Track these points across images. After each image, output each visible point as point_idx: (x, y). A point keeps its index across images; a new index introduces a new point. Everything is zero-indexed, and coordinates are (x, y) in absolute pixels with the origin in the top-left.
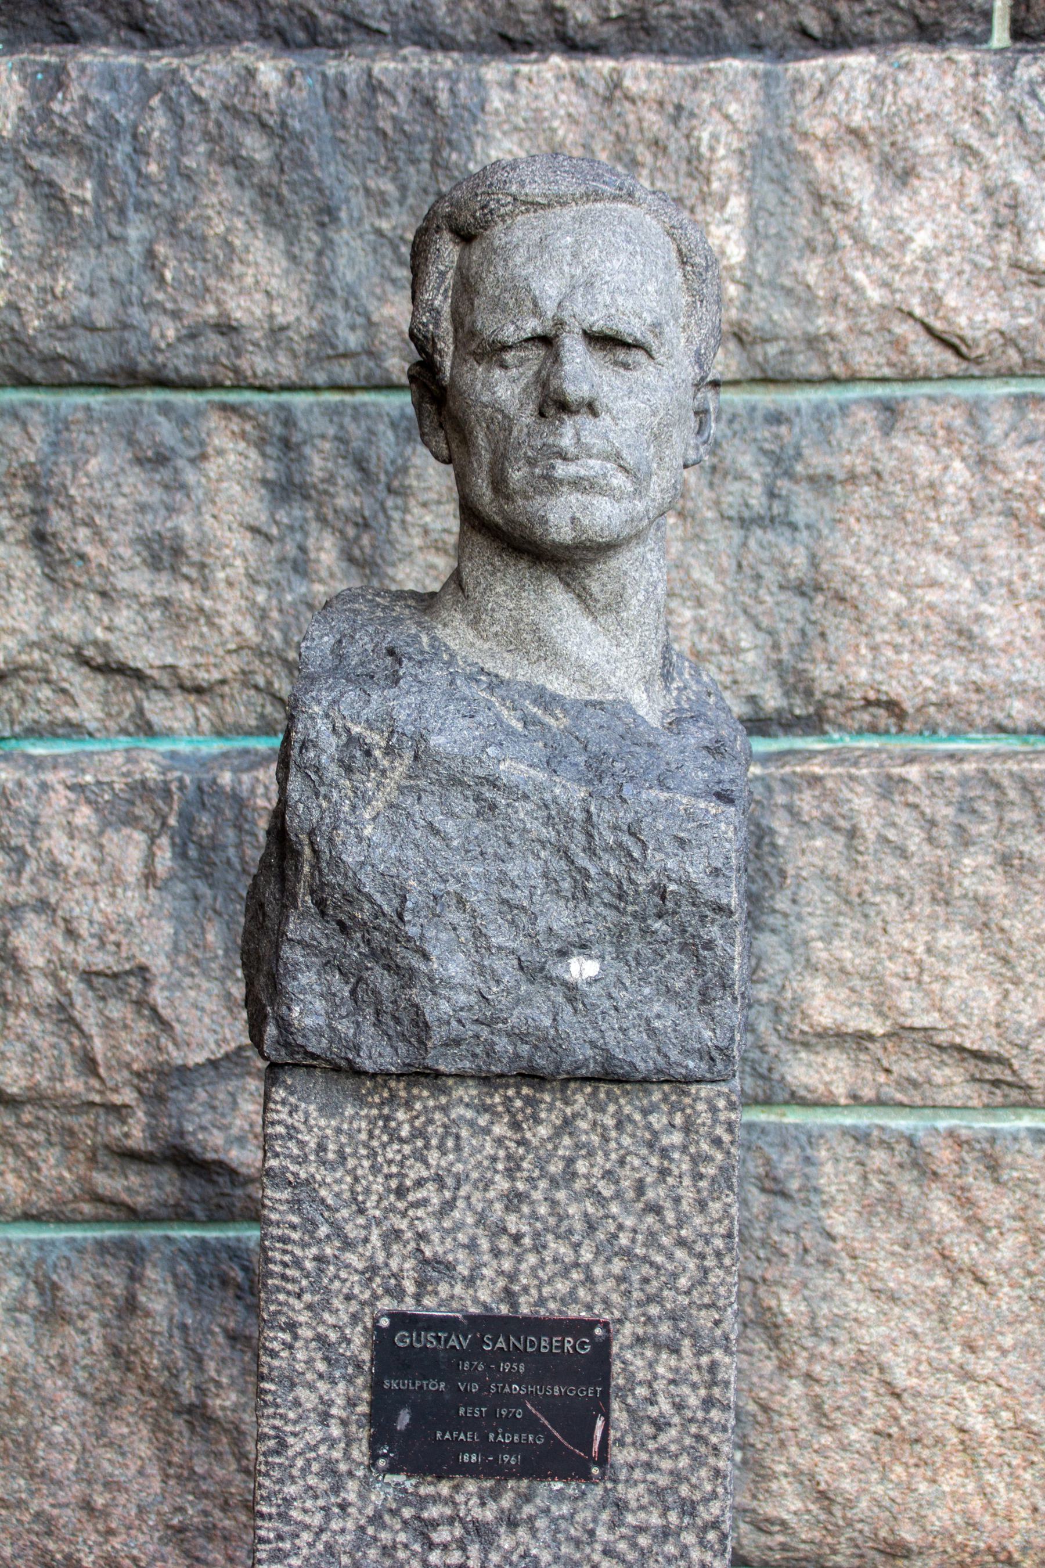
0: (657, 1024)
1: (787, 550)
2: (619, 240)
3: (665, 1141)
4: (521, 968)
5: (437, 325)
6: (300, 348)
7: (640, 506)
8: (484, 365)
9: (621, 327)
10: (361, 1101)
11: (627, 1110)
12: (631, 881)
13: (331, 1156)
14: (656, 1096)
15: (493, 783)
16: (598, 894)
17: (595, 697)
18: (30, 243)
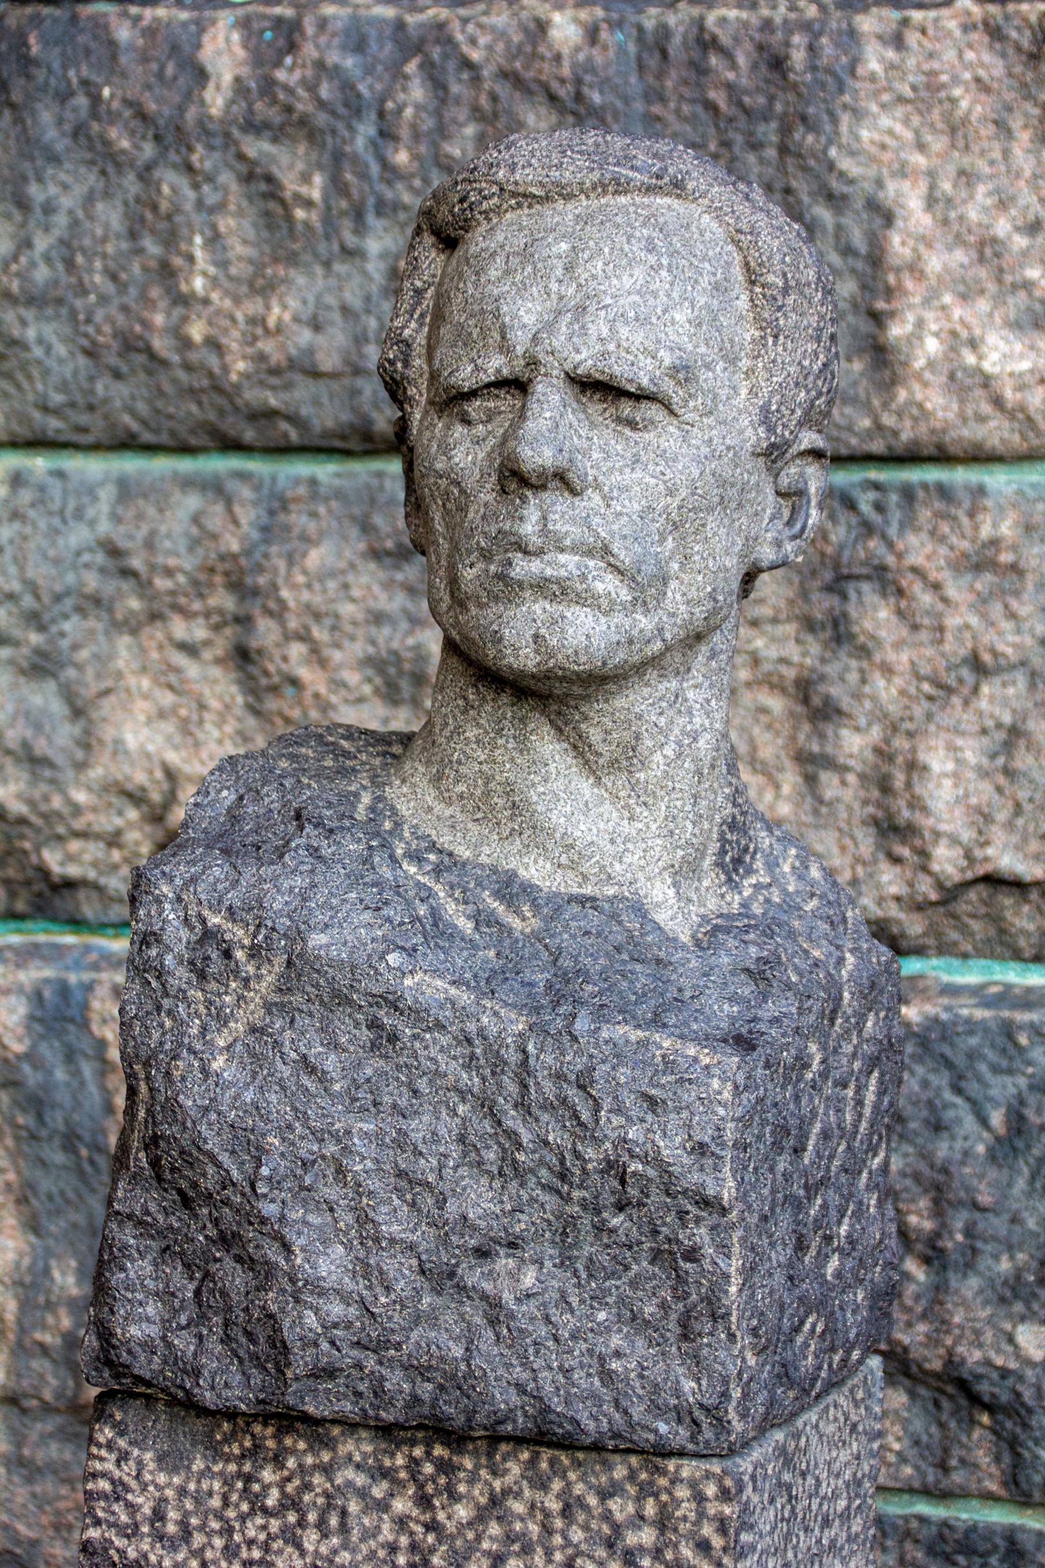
0: (615, 1365)
2: (636, 249)
3: (631, 1539)
4: (423, 1272)
5: (406, 364)
7: (645, 623)
8: (446, 419)
9: (617, 370)
10: (215, 1452)
11: (579, 1489)
12: (577, 1155)
13: (171, 1528)
14: (620, 1472)
15: (393, 1002)
16: (532, 1171)
17: (588, 890)
18: (240, 258)
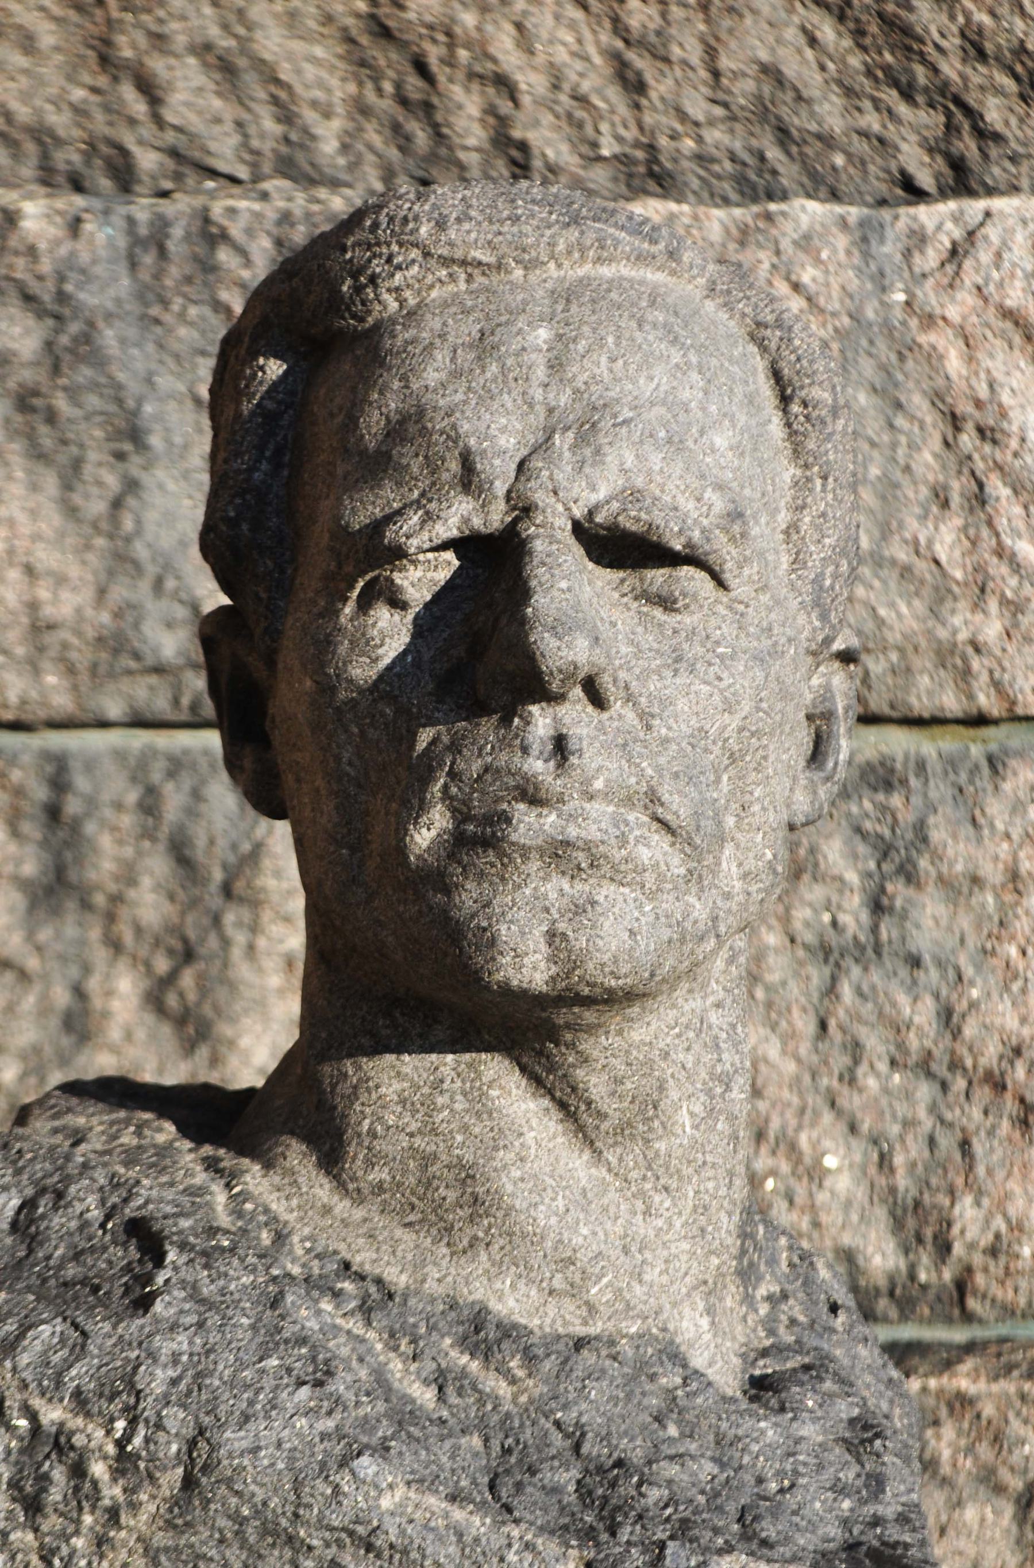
1: (903, 1000)
6: (82, 657)
17: (595, 1329)
